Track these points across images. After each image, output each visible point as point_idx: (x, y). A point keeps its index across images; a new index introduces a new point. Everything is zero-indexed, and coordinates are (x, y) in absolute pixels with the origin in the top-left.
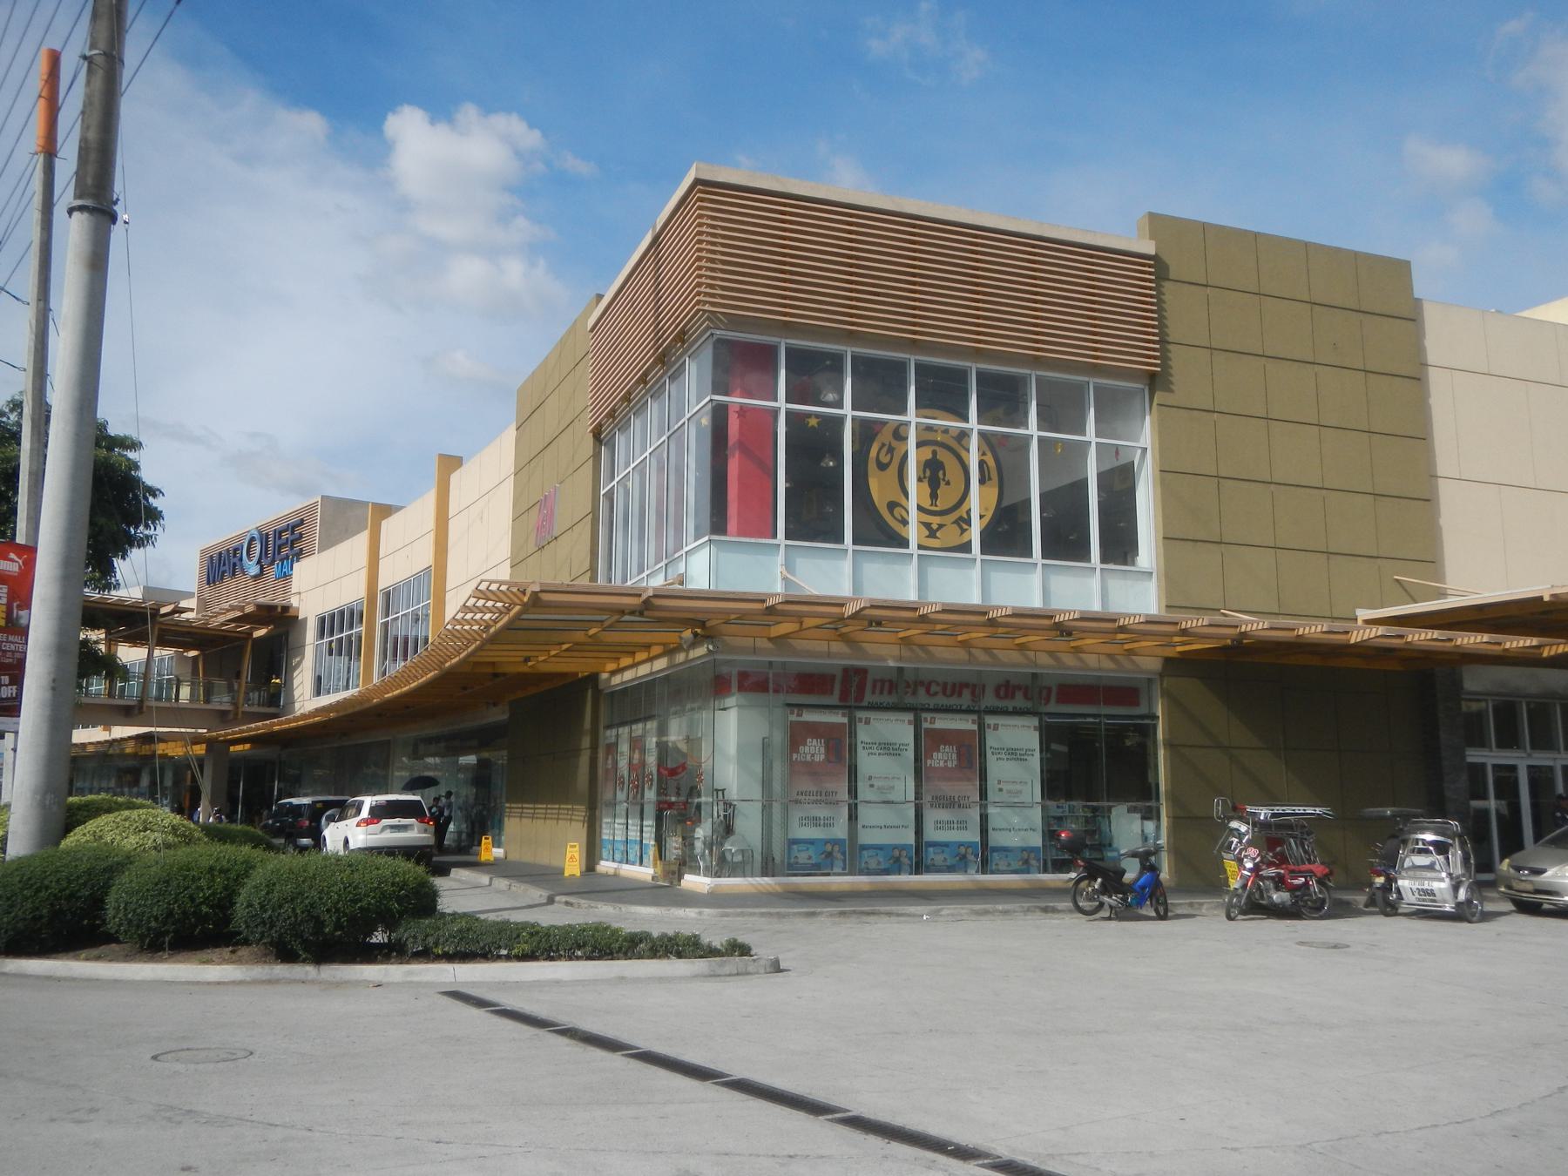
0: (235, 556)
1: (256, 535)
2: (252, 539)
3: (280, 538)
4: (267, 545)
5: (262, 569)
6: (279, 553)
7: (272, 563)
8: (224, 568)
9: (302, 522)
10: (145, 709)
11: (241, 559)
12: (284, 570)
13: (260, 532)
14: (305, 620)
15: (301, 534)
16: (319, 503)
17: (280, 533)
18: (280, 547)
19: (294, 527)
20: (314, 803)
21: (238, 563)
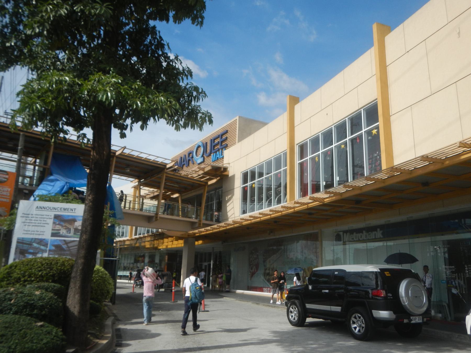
0: (189, 156)
1: (200, 144)
2: (199, 147)
3: (214, 142)
4: (206, 149)
5: (204, 159)
6: (214, 149)
7: (210, 155)
8: (184, 163)
9: (227, 132)
10: (158, 218)
11: (192, 157)
12: (217, 156)
13: (203, 144)
14: (233, 176)
15: (226, 138)
16: (238, 120)
17: (214, 140)
18: (214, 146)
19: (222, 135)
20: (382, 270)
21: (191, 159)
